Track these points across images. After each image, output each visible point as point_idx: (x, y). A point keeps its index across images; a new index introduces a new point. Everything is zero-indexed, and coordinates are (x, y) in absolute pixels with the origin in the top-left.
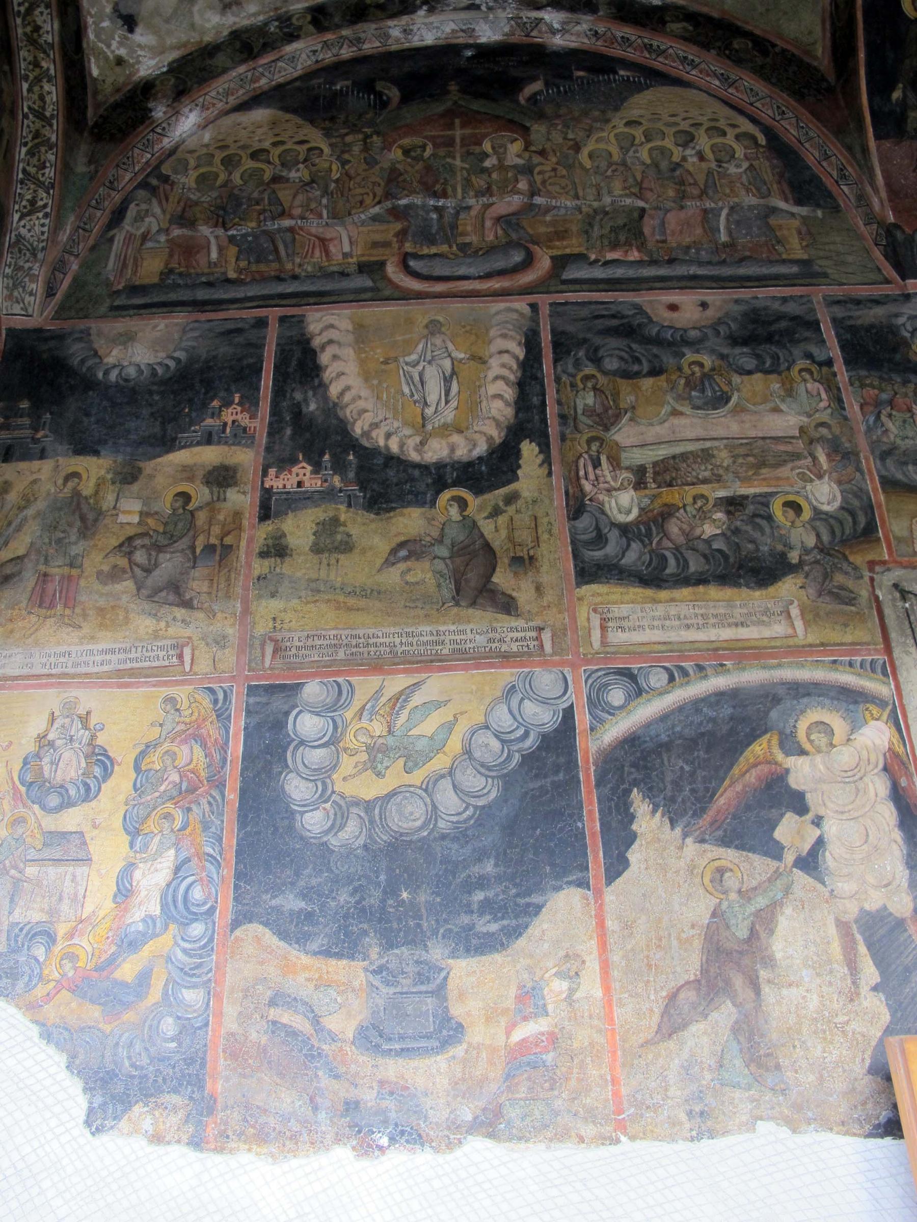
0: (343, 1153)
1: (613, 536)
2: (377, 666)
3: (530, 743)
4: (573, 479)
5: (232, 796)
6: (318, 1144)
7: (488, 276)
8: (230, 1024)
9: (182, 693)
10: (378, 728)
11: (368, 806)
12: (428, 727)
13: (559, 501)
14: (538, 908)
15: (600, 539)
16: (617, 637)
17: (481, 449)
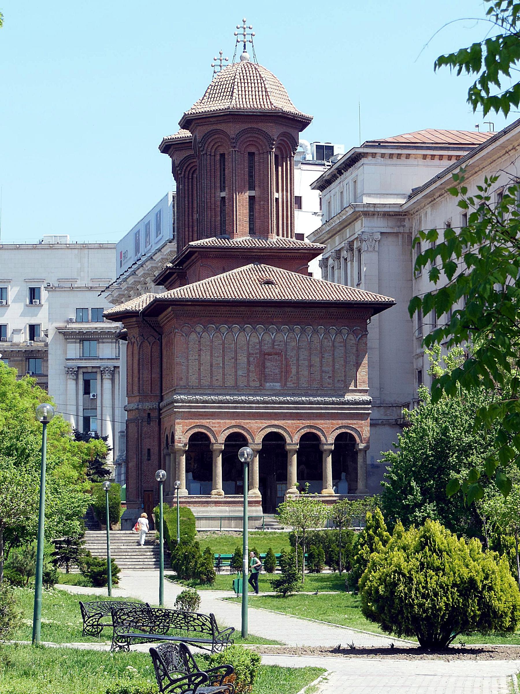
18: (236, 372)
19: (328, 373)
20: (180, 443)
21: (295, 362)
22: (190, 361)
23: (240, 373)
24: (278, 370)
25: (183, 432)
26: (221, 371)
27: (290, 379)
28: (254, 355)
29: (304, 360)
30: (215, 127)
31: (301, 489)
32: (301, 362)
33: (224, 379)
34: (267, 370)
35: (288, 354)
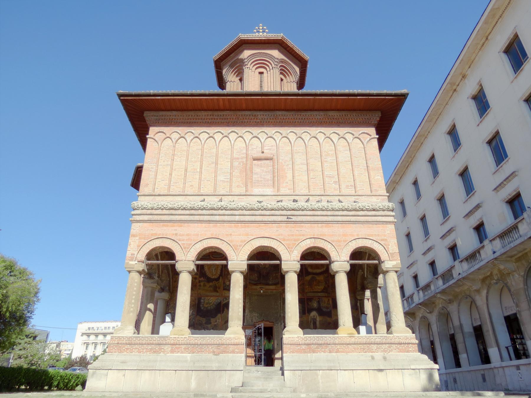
0: (203, 330)
1: (226, 286)
2: (207, 296)
3: (218, 303)
4: (224, 281)
5: (196, 306)
6: (202, 330)
7: (219, 258)
8: (196, 322)
9: (193, 298)
10: (207, 301)
11: (206, 307)
12: (211, 301)
13: (223, 283)
14: (217, 315)
15: (225, 286)
16: (225, 295)
17: (217, 277)
18: (216, 176)
19: (333, 177)
20: (131, 260)
21: (291, 166)
22: (159, 167)
23: (220, 178)
24: (269, 176)
25: (138, 246)
26: (198, 177)
27: (284, 185)
28: (240, 160)
29: (302, 164)
30: (233, 60)
31: (304, 325)
32: (296, 167)
33: (200, 184)
34: (255, 176)
35: (282, 158)
